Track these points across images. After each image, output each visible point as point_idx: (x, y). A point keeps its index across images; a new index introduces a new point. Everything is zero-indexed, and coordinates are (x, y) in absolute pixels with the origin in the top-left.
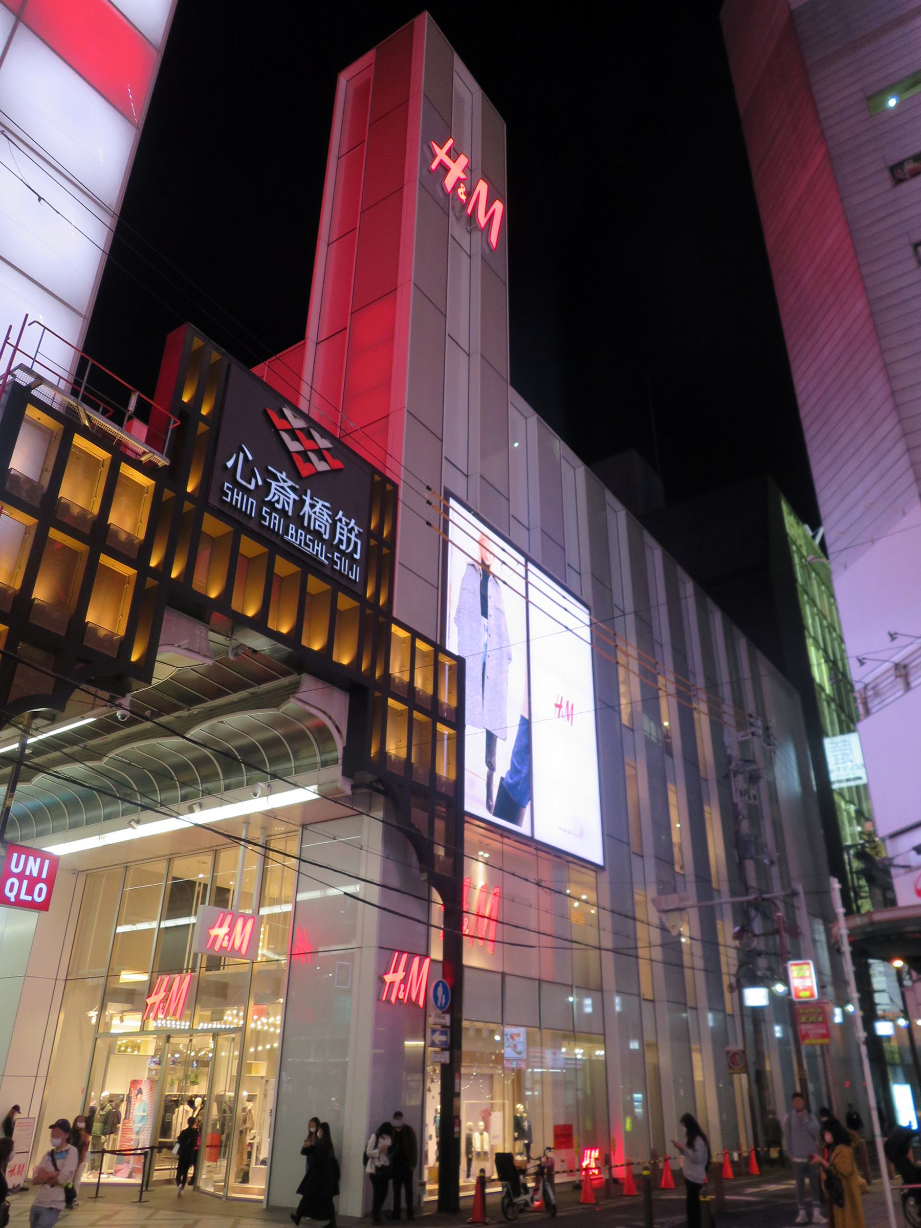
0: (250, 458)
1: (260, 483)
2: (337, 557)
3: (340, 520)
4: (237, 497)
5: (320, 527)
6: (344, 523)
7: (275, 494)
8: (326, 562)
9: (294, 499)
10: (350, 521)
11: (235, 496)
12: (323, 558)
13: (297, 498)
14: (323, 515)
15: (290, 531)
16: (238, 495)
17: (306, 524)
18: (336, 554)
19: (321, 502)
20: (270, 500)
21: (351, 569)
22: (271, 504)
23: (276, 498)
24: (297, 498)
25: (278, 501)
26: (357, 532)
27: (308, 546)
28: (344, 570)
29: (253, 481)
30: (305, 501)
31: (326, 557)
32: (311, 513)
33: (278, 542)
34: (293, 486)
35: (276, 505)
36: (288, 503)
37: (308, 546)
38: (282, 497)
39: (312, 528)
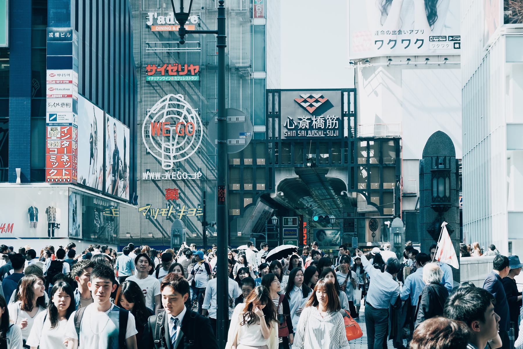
3: (328, 119)
6: (330, 119)
8: (324, 136)
11: (288, 133)
12: (323, 135)
13: (310, 121)
16: (289, 132)
17: (314, 128)
18: (327, 131)
19: (319, 117)
21: (334, 132)
22: (301, 129)
24: (310, 121)
25: (303, 127)
26: (336, 119)
27: (316, 134)
28: (332, 134)
29: (294, 125)
31: (324, 134)
33: (306, 138)
35: (303, 128)
36: (307, 125)
37: (316, 134)
38: (304, 124)
39: (317, 128)
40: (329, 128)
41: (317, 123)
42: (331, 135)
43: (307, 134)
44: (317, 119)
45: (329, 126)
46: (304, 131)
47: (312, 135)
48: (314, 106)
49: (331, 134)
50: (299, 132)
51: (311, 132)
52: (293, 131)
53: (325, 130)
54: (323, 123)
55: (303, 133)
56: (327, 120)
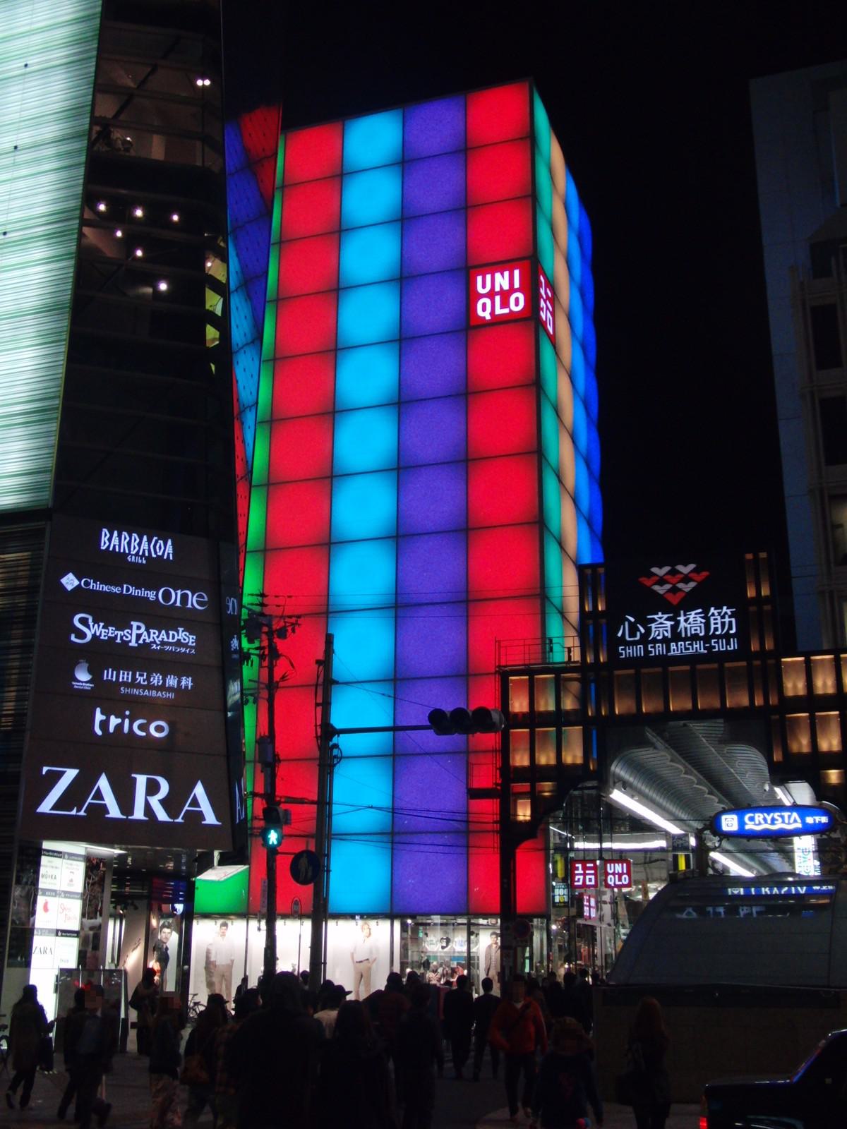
0: (632, 619)
1: (643, 631)
2: (715, 642)
3: (713, 615)
4: (630, 651)
5: (696, 630)
7: (655, 631)
8: (706, 651)
9: (671, 625)
10: (722, 609)
11: (628, 651)
12: (702, 650)
13: (672, 623)
14: (696, 621)
15: (672, 648)
16: (629, 649)
17: (683, 635)
18: (713, 641)
19: (693, 613)
20: (653, 638)
22: (655, 641)
23: (657, 633)
24: (672, 623)
25: (659, 635)
26: (729, 613)
27: (688, 649)
28: (723, 647)
29: (638, 634)
30: (679, 621)
32: (686, 625)
34: (668, 617)
35: (659, 638)
37: (688, 649)
38: (661, 629)
39: (689, 635)
40: (717, 633)
41: (689, 626)
42: (721, 649)
43: (668, 650)
44: (688, 616)
45: (716, 629)
46: (660, 645)
47: (680, 651)
48: (680, 590)
49: (720, 646)
50: (651, 647)
51: (677, 646)
52: (639, 646)
53: (707, 639)
54: (702, 625)
55: (659, 649)
56: (710, 617)
